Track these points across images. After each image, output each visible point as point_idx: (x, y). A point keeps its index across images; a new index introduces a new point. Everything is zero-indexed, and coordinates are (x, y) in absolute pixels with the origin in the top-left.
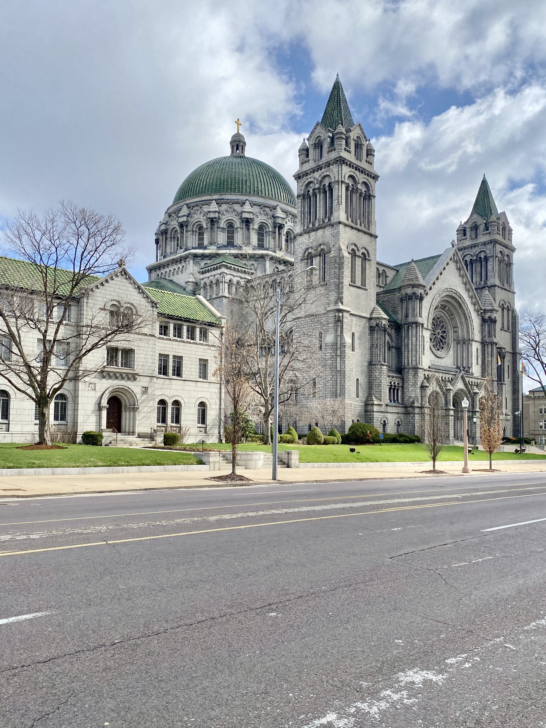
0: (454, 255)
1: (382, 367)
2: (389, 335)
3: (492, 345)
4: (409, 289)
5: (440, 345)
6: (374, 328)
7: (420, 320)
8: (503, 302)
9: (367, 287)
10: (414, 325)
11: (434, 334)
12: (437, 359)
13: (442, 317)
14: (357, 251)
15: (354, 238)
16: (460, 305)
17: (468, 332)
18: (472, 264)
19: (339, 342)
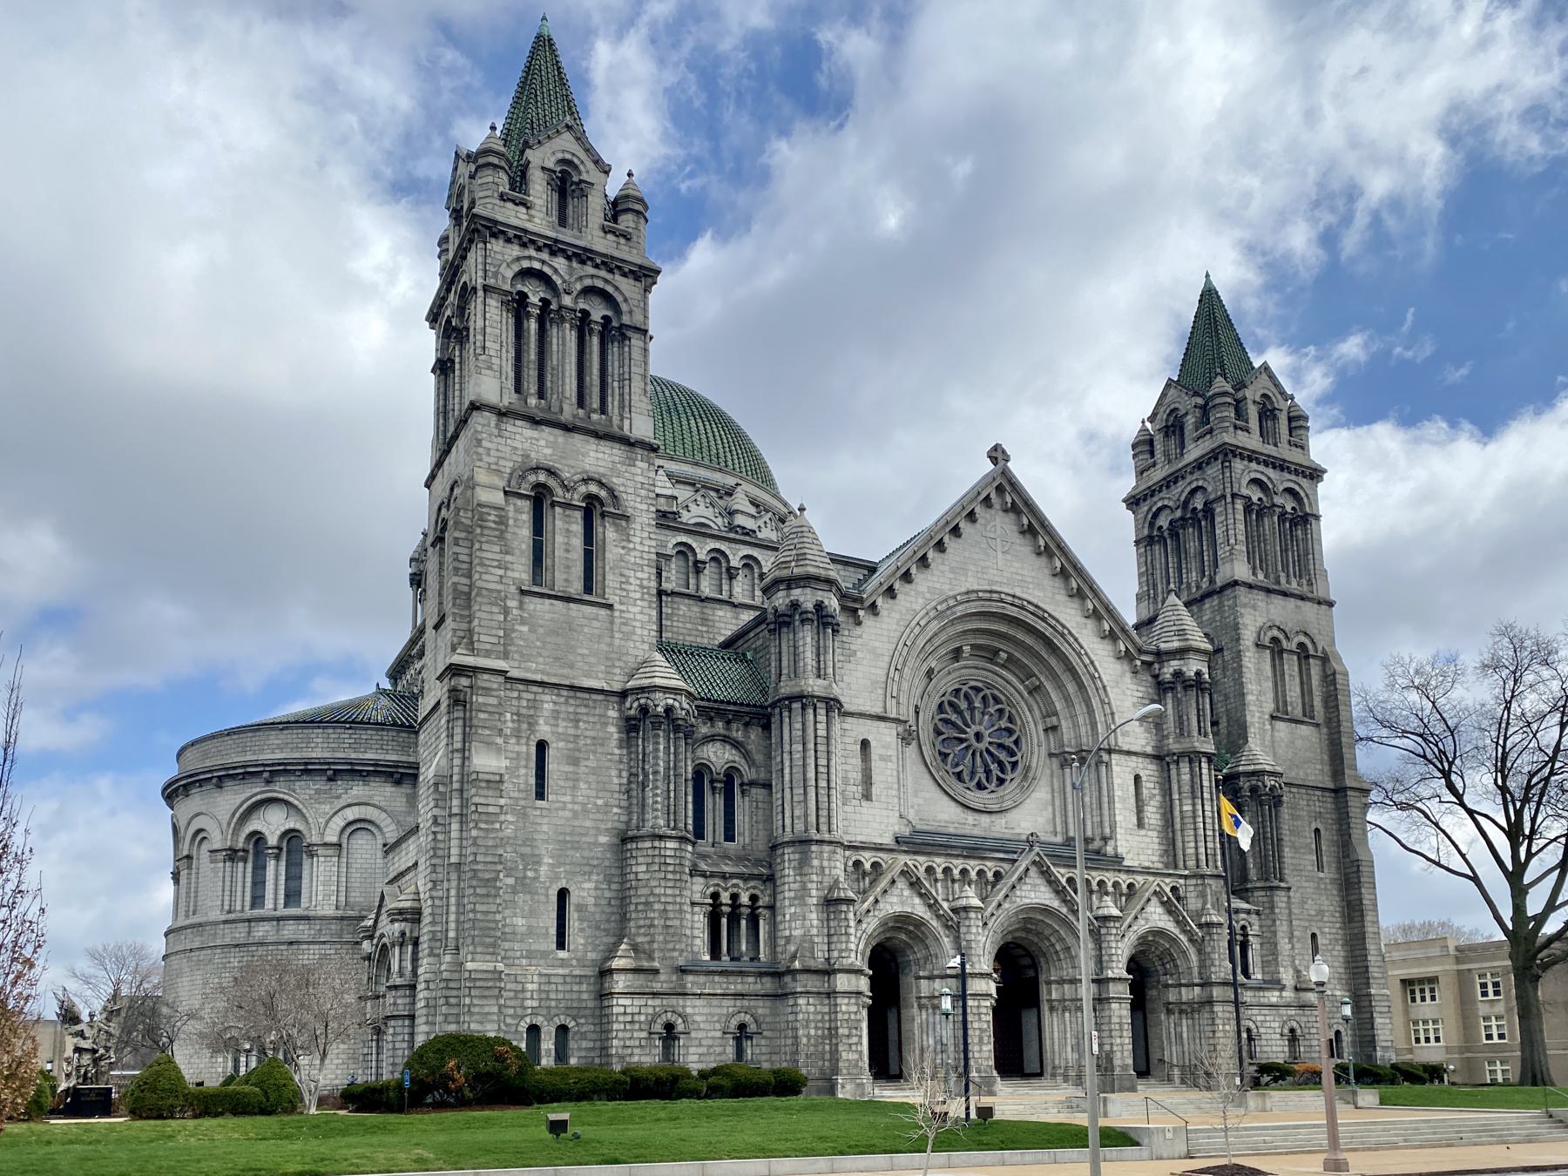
0: (1000, 489)
1: (657, 844)
2: (736, 745)
3: (1191, 761)
4: (781, 594)
5: (988, 772)
6: (640, 719)
7: (814, 685)
8: (1275, 633)
9: (612, 599)
10: (796, 706)
11: (961, 741)
12: (971, 818)
13: (989, 686)
14: (559, 491)
15: (548, 451)
16: (1049, 643)
17: (1094, 725)
18: (1177, 535)
19: (456, 770)
